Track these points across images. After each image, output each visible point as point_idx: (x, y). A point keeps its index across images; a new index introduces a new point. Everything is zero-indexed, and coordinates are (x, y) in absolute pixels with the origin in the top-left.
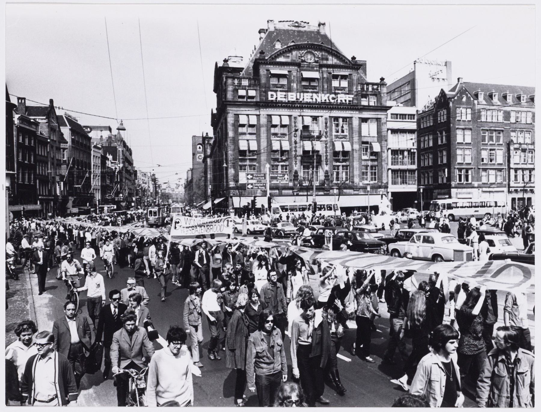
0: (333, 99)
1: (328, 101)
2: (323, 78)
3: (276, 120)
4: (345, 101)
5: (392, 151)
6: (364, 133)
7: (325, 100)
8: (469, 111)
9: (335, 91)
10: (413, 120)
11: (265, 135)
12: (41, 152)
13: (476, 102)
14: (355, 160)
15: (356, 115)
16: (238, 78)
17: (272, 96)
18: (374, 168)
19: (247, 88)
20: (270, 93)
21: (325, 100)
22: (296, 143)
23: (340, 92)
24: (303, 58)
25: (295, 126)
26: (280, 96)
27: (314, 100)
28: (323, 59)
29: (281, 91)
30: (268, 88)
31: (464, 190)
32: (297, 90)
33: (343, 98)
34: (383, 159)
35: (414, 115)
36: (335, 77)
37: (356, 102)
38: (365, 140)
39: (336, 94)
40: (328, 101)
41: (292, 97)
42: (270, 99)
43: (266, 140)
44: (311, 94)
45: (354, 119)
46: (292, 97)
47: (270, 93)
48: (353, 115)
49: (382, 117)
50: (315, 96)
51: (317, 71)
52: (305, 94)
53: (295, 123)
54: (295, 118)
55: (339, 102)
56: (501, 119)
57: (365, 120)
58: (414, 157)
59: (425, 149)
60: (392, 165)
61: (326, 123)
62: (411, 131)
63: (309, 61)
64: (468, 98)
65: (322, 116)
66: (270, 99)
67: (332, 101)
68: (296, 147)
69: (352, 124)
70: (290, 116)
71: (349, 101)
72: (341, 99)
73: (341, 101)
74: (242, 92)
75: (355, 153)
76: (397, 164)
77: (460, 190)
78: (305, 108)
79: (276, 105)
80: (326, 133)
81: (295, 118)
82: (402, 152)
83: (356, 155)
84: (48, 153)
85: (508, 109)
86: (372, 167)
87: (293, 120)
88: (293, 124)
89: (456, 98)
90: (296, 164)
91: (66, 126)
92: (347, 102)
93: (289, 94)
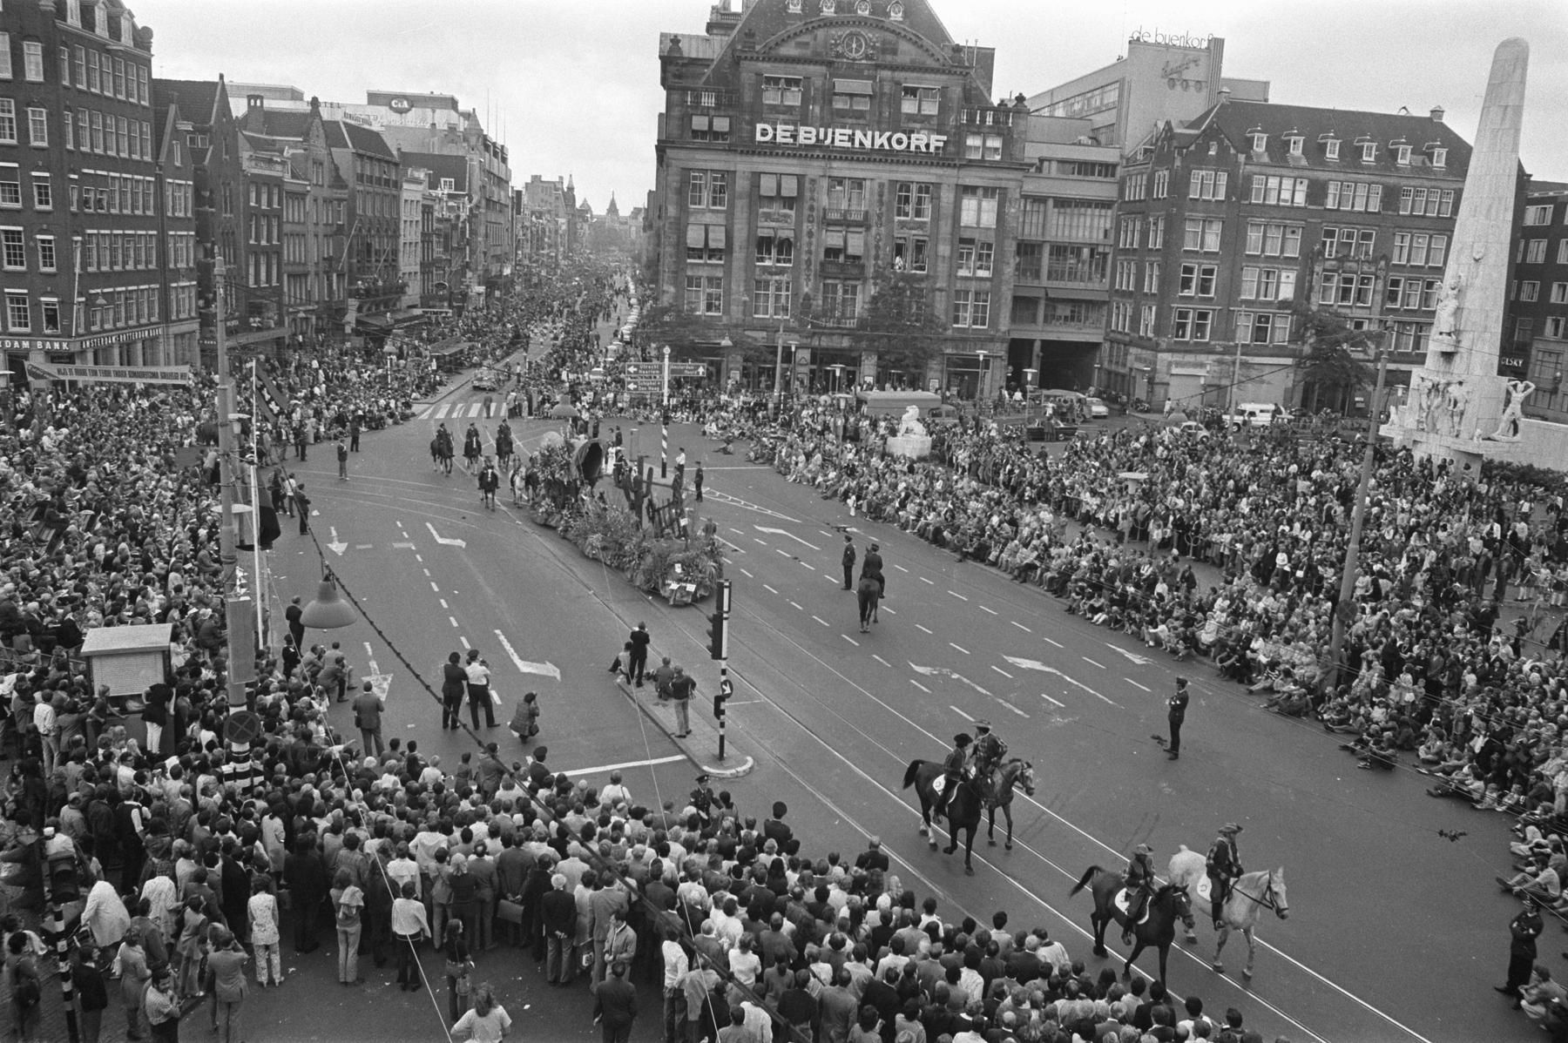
0: (899, 142)
1: (887, 147)
2: (883, 94)
3: (768, 186)
4: (927, 146)
5: (1052, 247)
6: (968, 217)
8: (1223, 178)
9: (906, 125)
10: (1109, 179)
11: (745, 215)
12: (291, 213)
13: (1242, 158)
15: (949, 177)
16: (693, 90)
17: (763, 132)
18: (983, 297)
19: (712, 113)
22: (810, 234)
23: (918, 126)
24: (839, 49)
25: (812, 199)
26: (782, 134)
27: (857, 144)
28: (884, 51)
29: (786, 123)
30: (758, 112)
31: (1190, 358)
32: (822, 118)
33: (920, 139)
35: (1114, 166)
36: (912, 92)
38: (967, 235)
39: (909, 132)
40: (887, 147)
41: (807, 135)
42: (759, 138)
43: (746, 227)
44: (850, 132)
45: (944, 187)
47: (759, 127)
48: (945, 180)
49: (1011, 185)
51: (868, 78)
52: (838, 131)
53: (812, 191)
54: (813, 181)
55: (913, 148)
56: (1300, 199)
57: (970, 190)
58: (1105, 262)
59: (1125, 251)
60: (1049, 278)
61: (881, 195)
62: (1104, 205)
63: (853, 55)
64: (1223, 150)
67: (896, 147)
68: (810, 244)
69: (939, 198)
70: (800, 178)
71: (937, 148)
73: (917, 147)
74: (700, 123)
76: (1062, 278)
77: (1177, 357)
79: (772, 150)
80: (879, 216)
82: (1076, 250)
84: (306, 214)
85: (1321, 175)
86: (977, 294)
88: (808, 194)
89: (1192, 148)
90: (808, 279)
91: (346, 146)
92: (932, 149)
93: (802, 129)
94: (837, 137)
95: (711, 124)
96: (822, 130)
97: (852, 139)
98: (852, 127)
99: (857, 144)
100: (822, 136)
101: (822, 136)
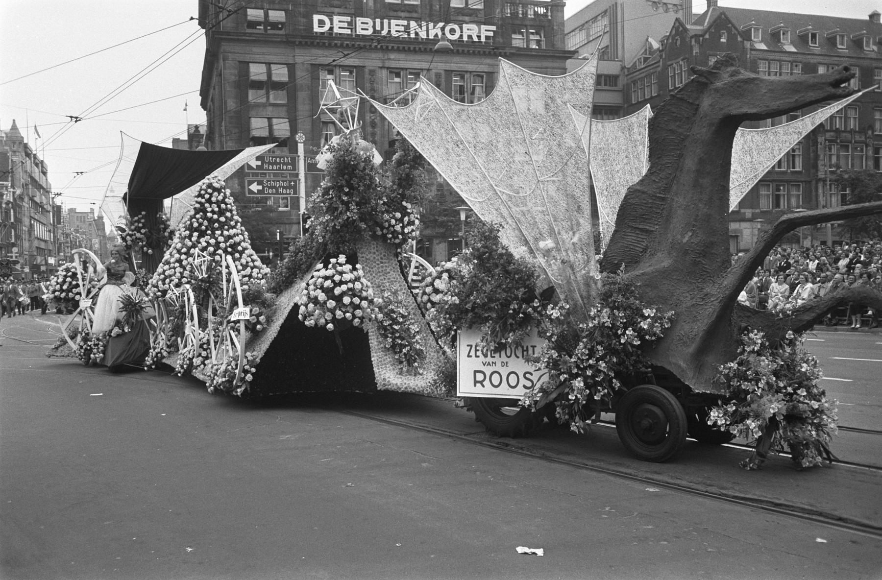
7: (436, 35)
20: (316, 18)
21: (436, 35)
26: (339, 24)
44: (405, 23)
46: (365, 26)
47: (316, 18)
50: (413, 24)
52: (394, 22)
54: (372, 72)
55: (465, 38)
72: (469, 33)
78: (393, 50)
81: (372, 72)
87: (367, 76)
93: (359, 20)
94: (393, 25)
95: (266, 15)
96: (378, 21)
97: (407, 28)
98: (408, 19)
100: (378, 28)
101: (378, 28)
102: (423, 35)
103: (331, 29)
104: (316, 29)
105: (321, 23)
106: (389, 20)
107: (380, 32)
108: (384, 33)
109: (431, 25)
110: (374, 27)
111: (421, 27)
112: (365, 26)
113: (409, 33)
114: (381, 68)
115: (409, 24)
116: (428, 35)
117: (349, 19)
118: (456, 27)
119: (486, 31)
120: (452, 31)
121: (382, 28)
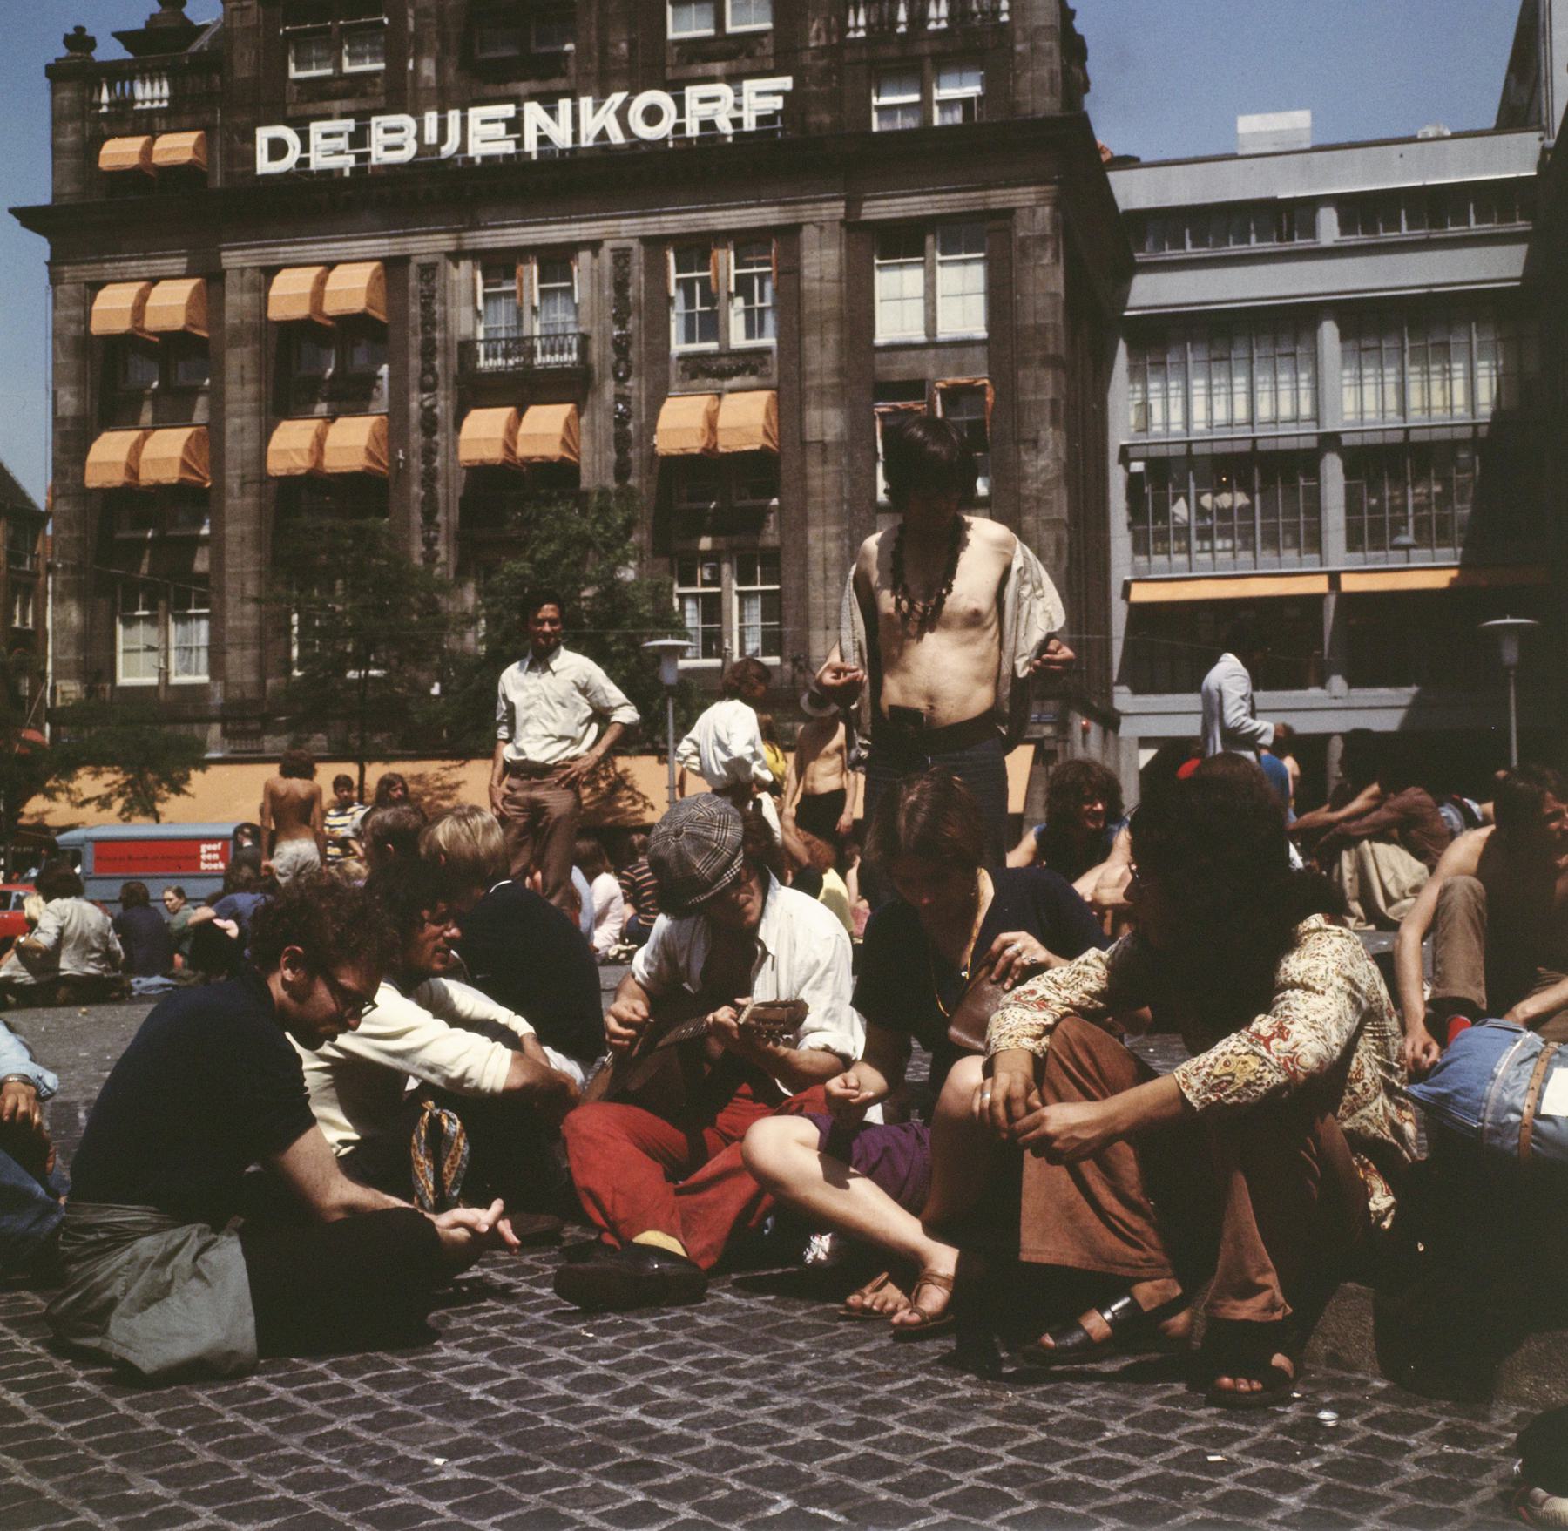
7: (603, 134)
14: (814, 513)
21: (603, 134)
22: (429, 423)
26: (326, 147)
27: (531, 145)
34: (1030, 487)
37: (826, 119)
40: (617, 137)
41: (394, 140)
46: (394, 139)
47: (264, 135)
50: (534, 113)
54: (429, 271)
55: (693, 130)
61: (621, 285)
65: (594, 246)
66: (264, 165)
72: (706, 111)
75: (814, 469)
81: (429, 271)
83: (822, 478)
87: (414, 283)
93: (378, 123)
96: (431, 118)
99: (531, 145)
101: (431, 136)
102: (561, 136)
103: (303, 162)
104: (264, 165)
105: (278, 149)
106: (464, 110)
107: (436, 149)
108: (449, 148)
109: (586, 102)
110: (419, 136)
111: (552, 112)
112: (394, 139)
113: (519, 143)
114: (456, 256)
115: (520, 113)
116: (576, 136)
117: (349, 125)
118: (663, 99)
119: (760, 98)
120: (653, 115)
121: (443, 137)
